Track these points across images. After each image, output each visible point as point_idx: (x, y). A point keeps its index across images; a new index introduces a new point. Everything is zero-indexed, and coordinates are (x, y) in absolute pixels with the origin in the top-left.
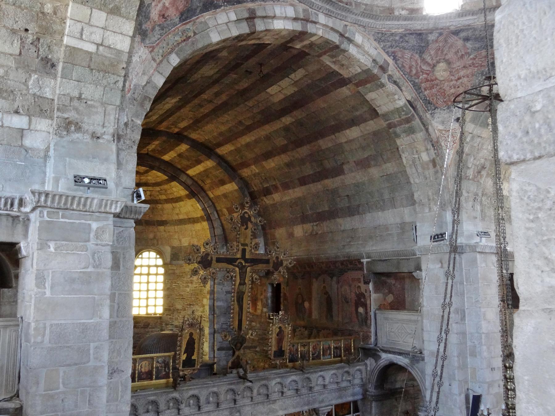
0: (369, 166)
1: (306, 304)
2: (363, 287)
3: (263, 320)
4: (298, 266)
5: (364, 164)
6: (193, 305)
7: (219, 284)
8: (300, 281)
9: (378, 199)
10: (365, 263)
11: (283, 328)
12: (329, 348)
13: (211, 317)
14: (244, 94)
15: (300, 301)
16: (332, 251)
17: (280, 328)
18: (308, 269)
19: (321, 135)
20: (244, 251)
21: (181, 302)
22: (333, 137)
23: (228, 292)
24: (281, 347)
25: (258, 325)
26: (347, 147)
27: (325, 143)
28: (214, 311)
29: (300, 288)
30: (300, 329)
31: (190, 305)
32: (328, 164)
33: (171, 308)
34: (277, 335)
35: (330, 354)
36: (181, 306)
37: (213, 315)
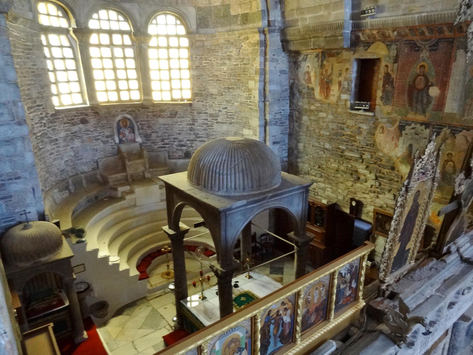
1: (434, 92)
3: (339, 110)
4: (425, 29)
6: (233, 88)
7: (272, 60)
8: (425, 54)
13: (262, 105)
15: (420, 84)
18: (447, 34)
21: (214, 84)
23: (282, 72)
25: (331, 117)
28: (265, 97)
29: (423, 66)
30: (413, 125)
31: (229, 88)
33: (204, 93)
36: (217, 90)
37: (264, 102)
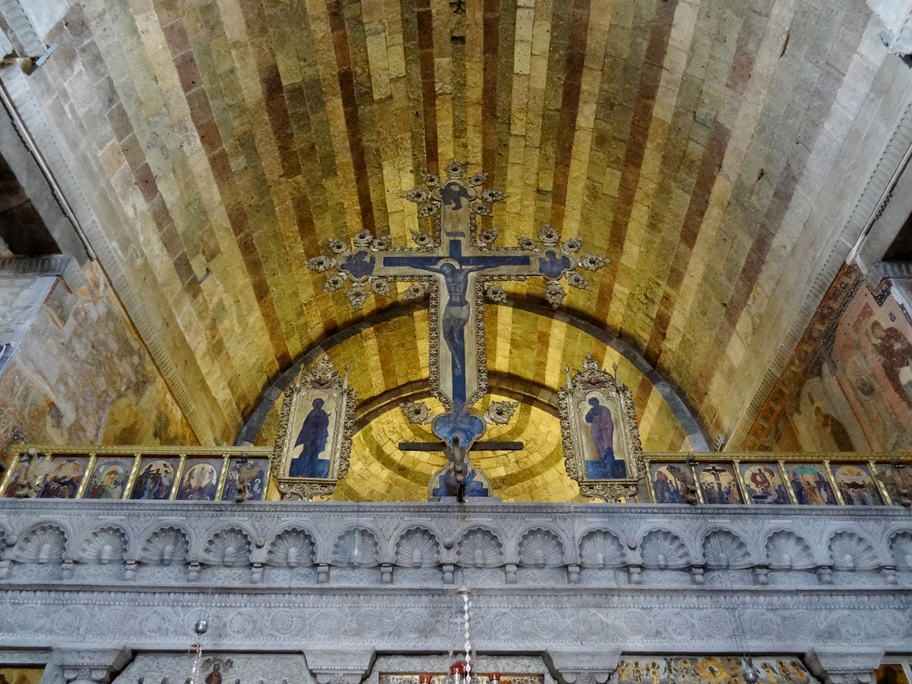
0: (751, 62)
2: (881, 315)
5: (742, 70)
9: (805, 106)
10: (859, 261)
11: (603, 403)
12: (823, 484)
14: (493, 107)
16: (791, 318)
17: (594, 401)
19: (648, 93)
20: (455, 246)
22: (664, 74)
24: (610, 451)
26: (698, 73)
27: (664, 107)
32: (697, 150)
34: (589, 418)
35: (832, 500)
